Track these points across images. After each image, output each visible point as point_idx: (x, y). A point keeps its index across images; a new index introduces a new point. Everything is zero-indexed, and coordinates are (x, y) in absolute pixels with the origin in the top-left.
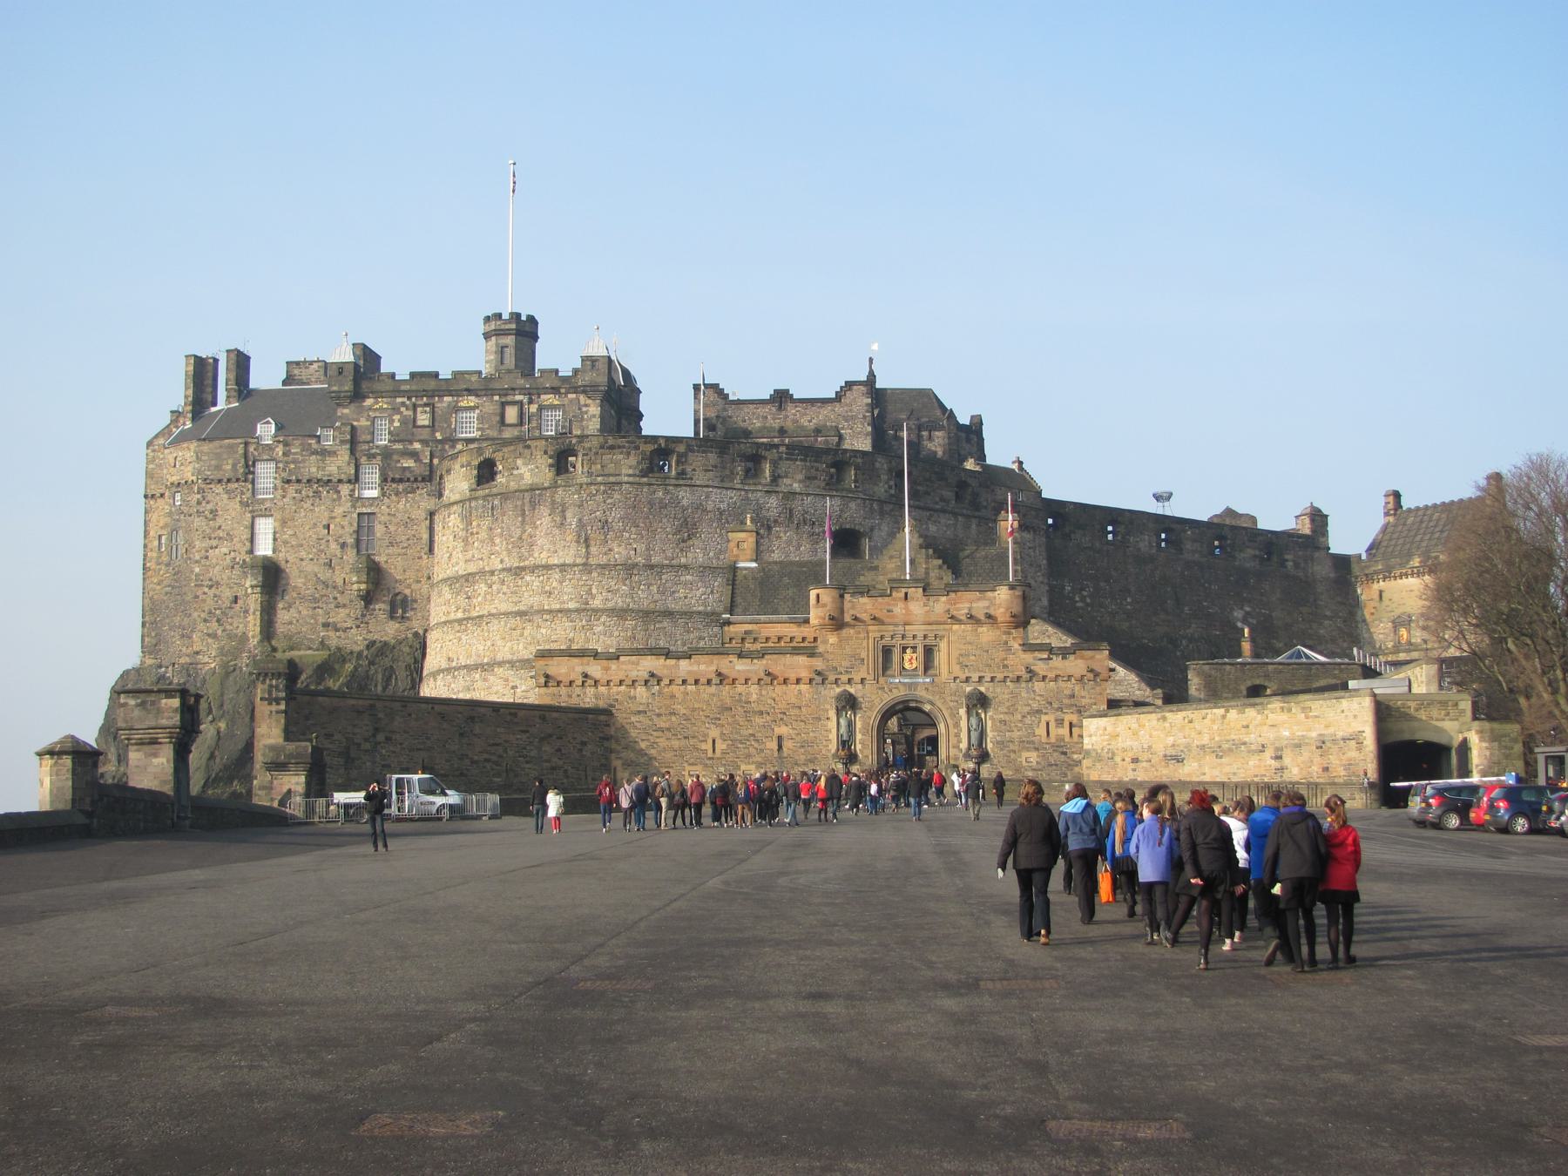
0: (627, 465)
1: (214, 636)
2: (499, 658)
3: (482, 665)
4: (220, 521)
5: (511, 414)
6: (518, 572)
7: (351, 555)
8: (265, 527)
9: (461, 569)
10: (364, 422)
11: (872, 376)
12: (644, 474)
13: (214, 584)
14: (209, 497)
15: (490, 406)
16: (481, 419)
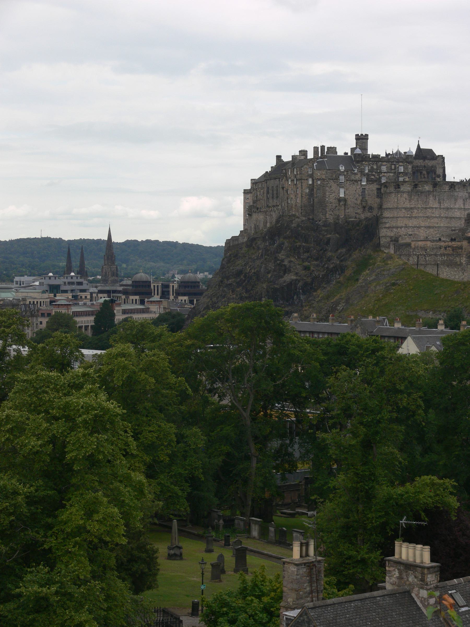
0: (447, 188)
1: (331, 215)
2: (422, 225)
3: (417, 227)
4: (332, 188)
5: (393, 167)
6: (426, 208)
7: (361, 198)
8: (342, 191)
9: (408, 206)
10: (363, 167)
11: (419, 146)
12: (450, 189)
13: (331, 203)
14: (330, 183)
15: (389, 165)
16: (387, 167)
